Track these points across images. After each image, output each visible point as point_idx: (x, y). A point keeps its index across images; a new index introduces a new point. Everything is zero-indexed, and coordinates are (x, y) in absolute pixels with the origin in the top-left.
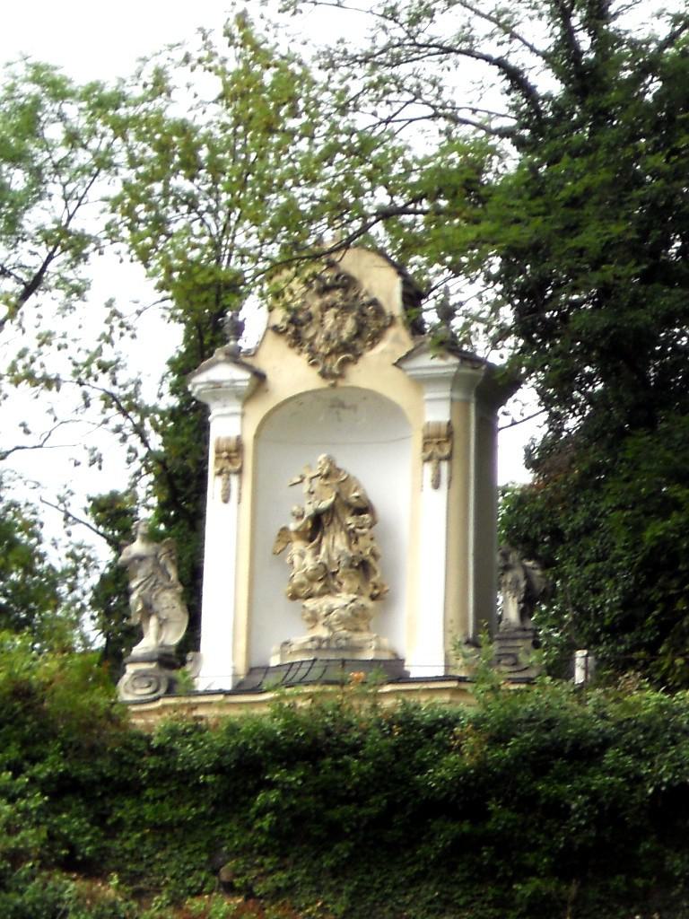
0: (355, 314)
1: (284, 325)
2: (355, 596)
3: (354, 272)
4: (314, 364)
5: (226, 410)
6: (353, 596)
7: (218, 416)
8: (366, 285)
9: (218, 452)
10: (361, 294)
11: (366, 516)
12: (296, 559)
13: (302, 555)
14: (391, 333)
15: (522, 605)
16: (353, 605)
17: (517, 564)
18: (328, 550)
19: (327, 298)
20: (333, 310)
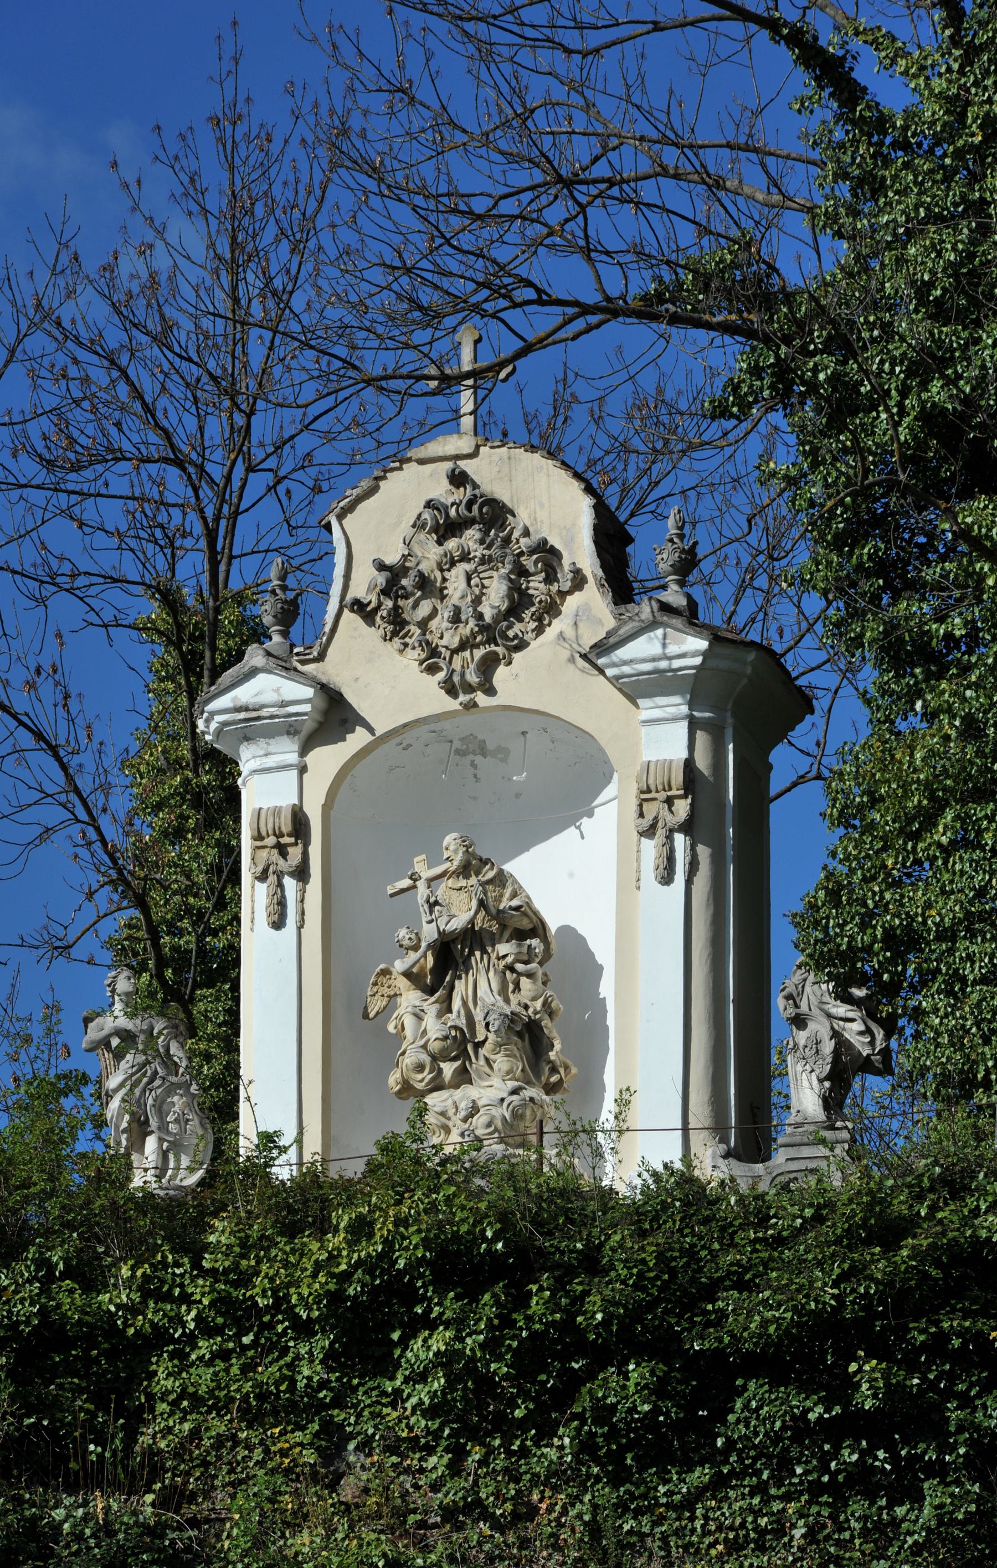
1: (373, 598)
2: (516, 1084)
3: (503, 494)
4: (432, 670)
5: (271, 761)
6: (512, 1084)
8: (523, 516)
9: (258, 837)
10: (516, 534)
11: (535, 942)
12: (409, 1021)
14: (572, 603)
16: (514, 1097)
17: (815, 1011)
18: (465, 1003)
19: (452, 544)
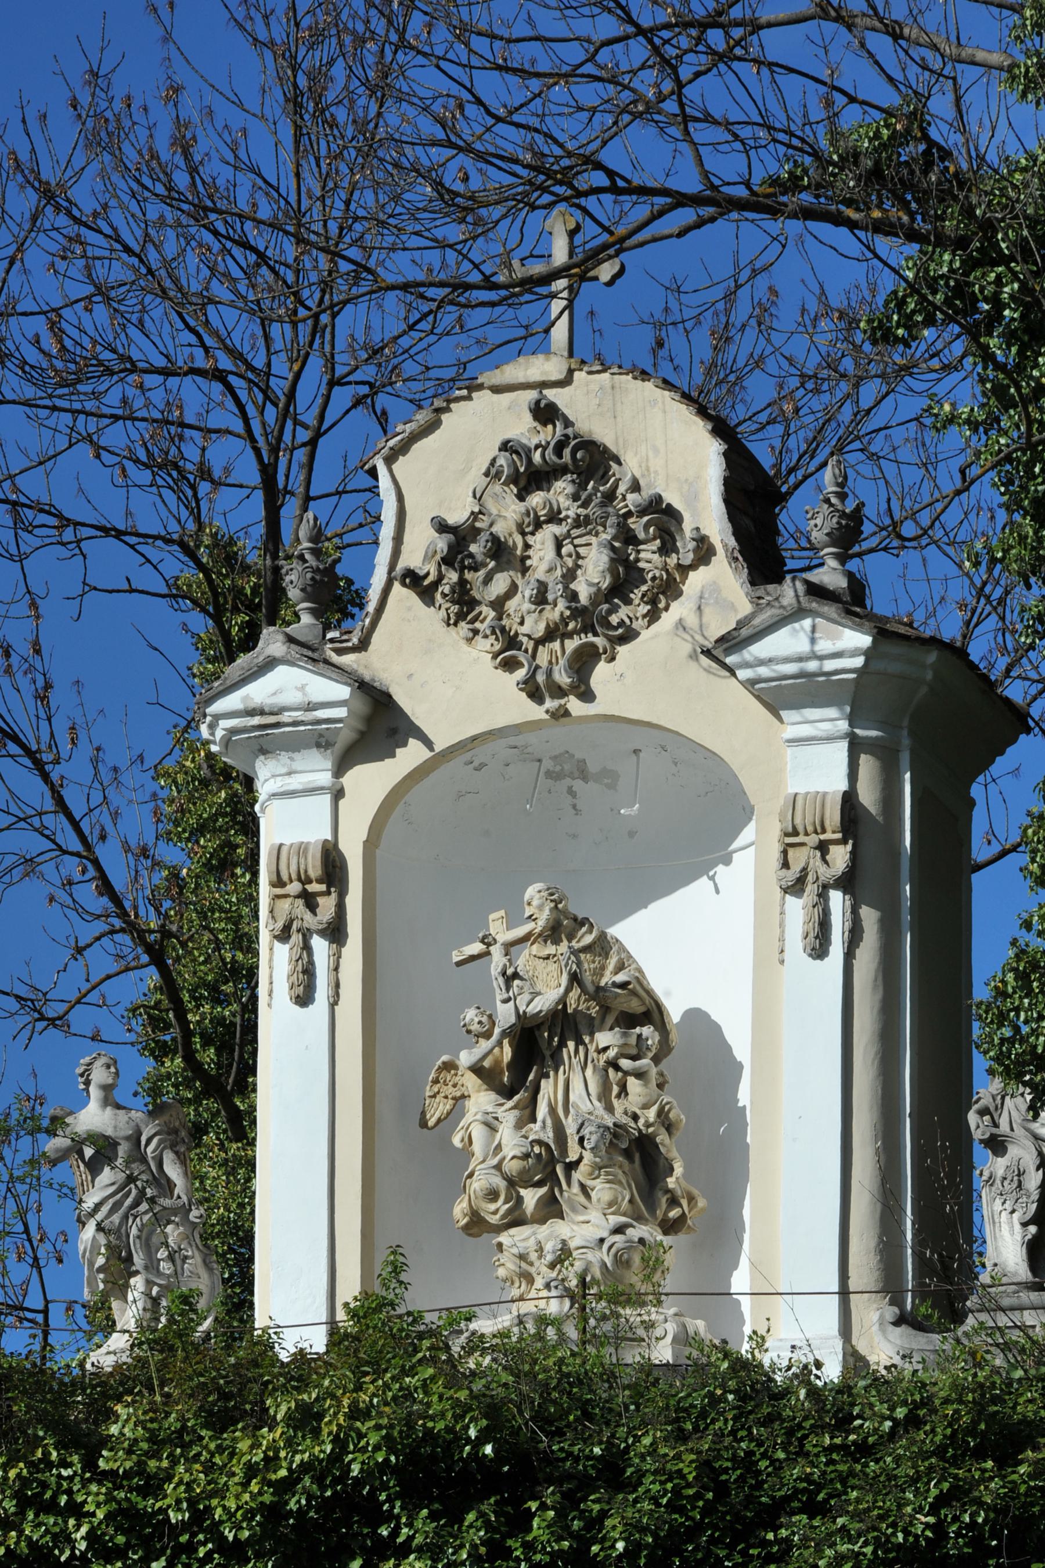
0: (605, 537)
1: (432, 569)
2: (623, 1219)
3: (604, 435)
4: (509, 665)
5: (296, 782)
6: (615, 1220)
7: (274, 795)
8: (632, 464)
9: (278, 882)
10: (622, 489)
11: (647, 1031)
12: (478, 1133)
13: (491, 1126)
14: (696, 581)
15: (1033, 1229)
16: (618, 1238)
17: (1019, 1132)
18: (552, 1110)
19: (536, 499)
20: (552, 530)
